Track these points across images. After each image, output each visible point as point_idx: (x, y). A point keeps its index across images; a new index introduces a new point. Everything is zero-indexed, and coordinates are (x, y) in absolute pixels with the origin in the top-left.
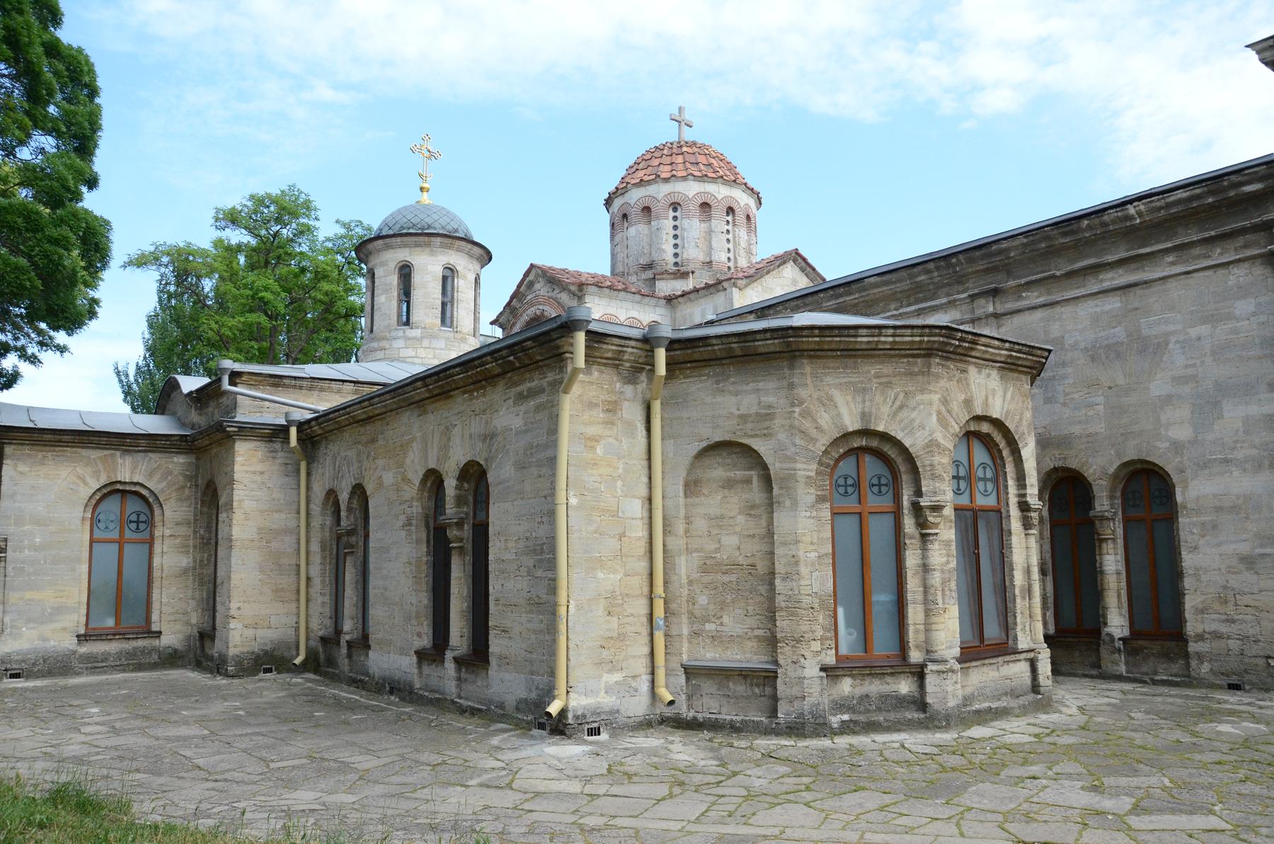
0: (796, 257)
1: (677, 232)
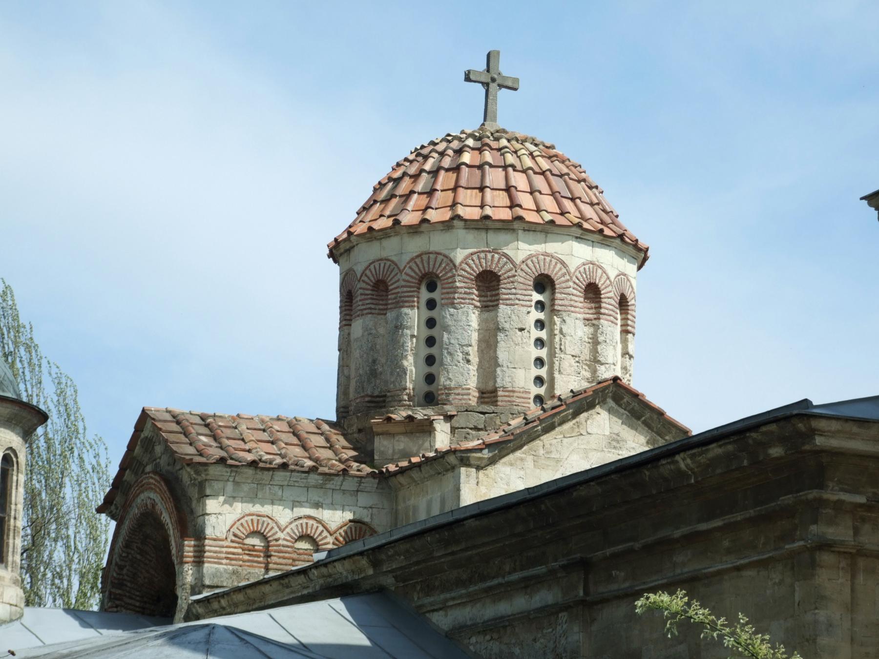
0: (618, 396)
1: (434, 332)
